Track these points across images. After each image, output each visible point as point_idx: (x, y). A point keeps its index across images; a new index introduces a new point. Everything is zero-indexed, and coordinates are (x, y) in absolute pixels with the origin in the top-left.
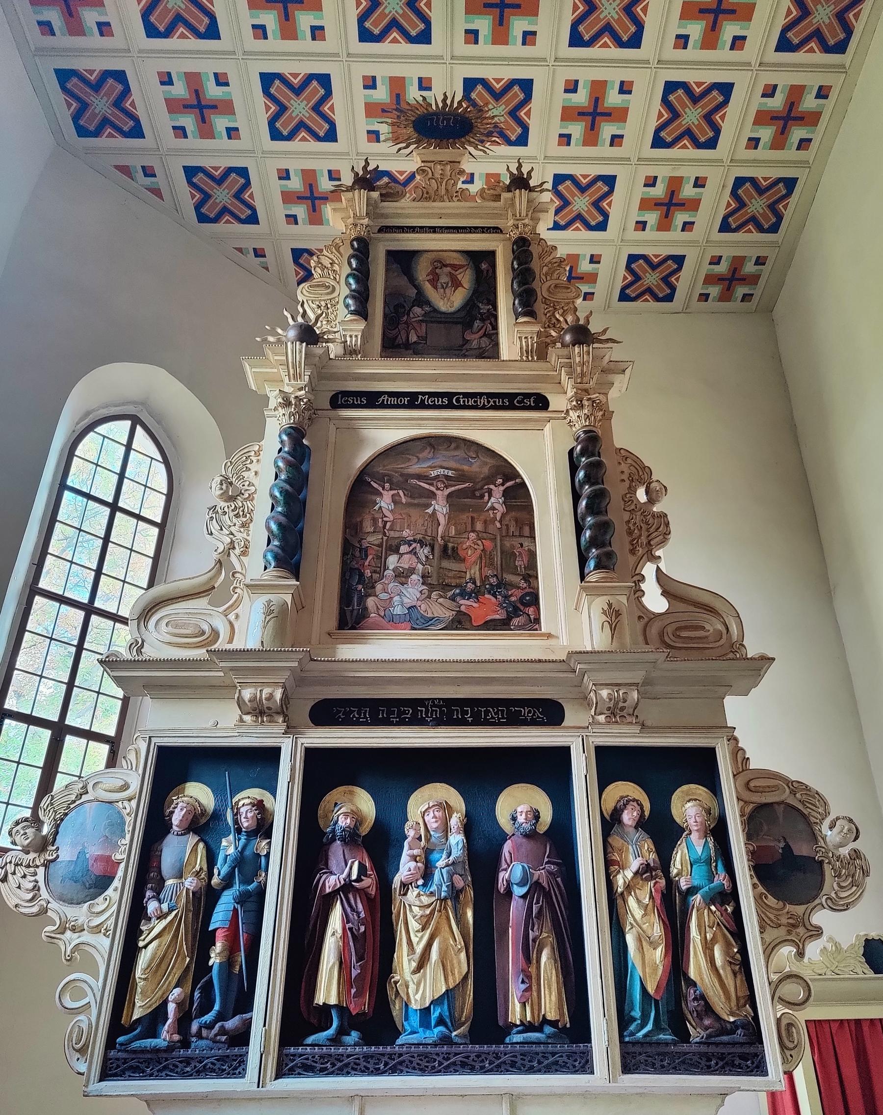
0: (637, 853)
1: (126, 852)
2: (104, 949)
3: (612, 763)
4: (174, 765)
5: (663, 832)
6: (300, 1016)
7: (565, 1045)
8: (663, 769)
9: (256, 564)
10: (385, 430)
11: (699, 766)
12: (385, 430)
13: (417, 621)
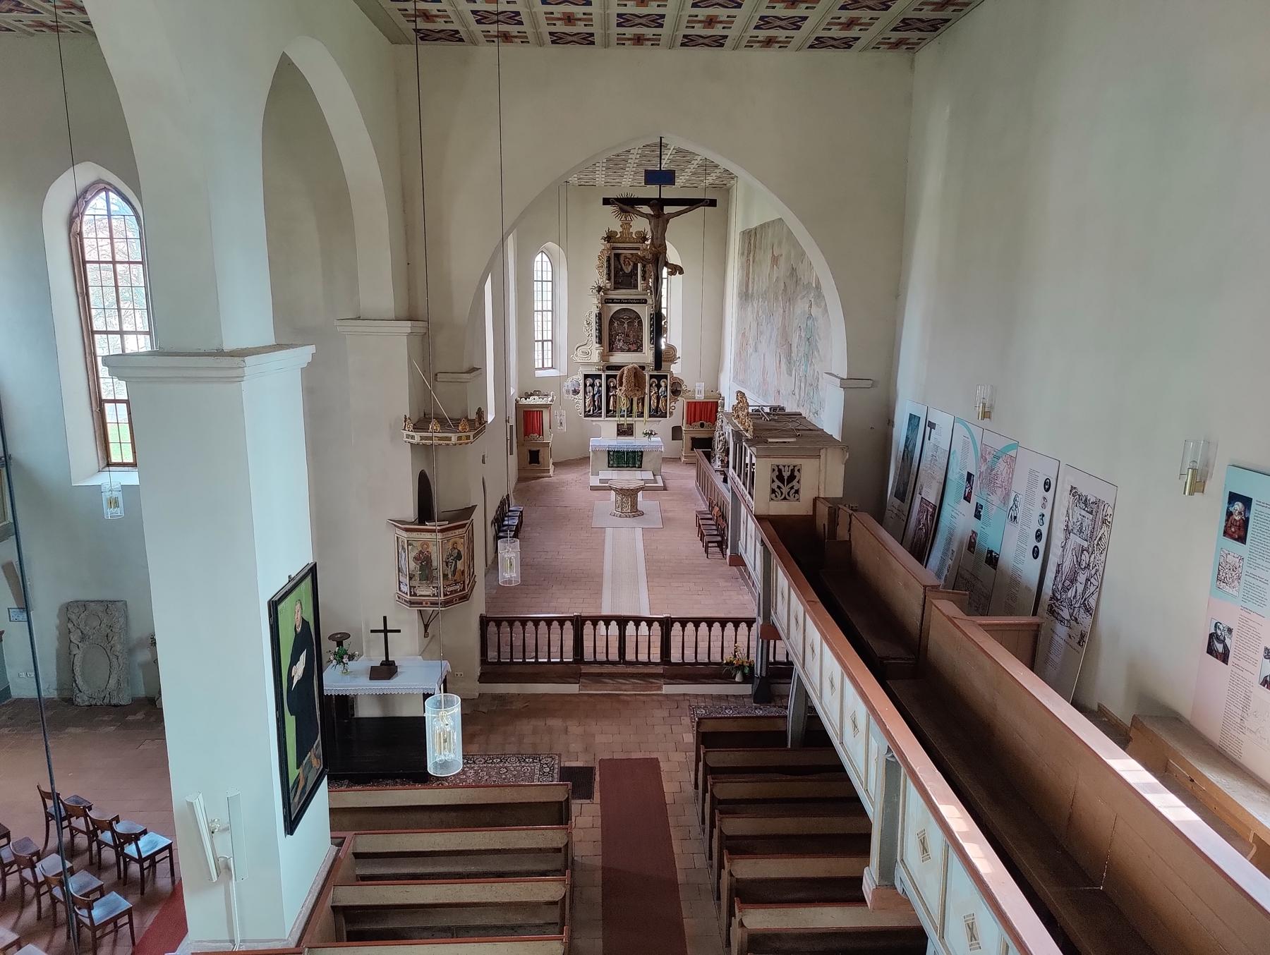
0: (655, 390)
1: (582, 387)
2: (582, 402)
3: (652, 377)
4: (586, 376)
5: (659, 386)
6: (608, 411)
7: (641, 415)
8: (659, 378)
9: (594, 339)
10: (616, 307)
11: (666, 377)
12: (616, 307)
13: (622, 350)
